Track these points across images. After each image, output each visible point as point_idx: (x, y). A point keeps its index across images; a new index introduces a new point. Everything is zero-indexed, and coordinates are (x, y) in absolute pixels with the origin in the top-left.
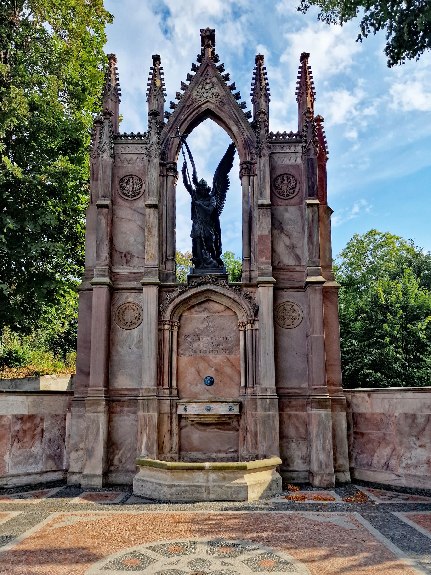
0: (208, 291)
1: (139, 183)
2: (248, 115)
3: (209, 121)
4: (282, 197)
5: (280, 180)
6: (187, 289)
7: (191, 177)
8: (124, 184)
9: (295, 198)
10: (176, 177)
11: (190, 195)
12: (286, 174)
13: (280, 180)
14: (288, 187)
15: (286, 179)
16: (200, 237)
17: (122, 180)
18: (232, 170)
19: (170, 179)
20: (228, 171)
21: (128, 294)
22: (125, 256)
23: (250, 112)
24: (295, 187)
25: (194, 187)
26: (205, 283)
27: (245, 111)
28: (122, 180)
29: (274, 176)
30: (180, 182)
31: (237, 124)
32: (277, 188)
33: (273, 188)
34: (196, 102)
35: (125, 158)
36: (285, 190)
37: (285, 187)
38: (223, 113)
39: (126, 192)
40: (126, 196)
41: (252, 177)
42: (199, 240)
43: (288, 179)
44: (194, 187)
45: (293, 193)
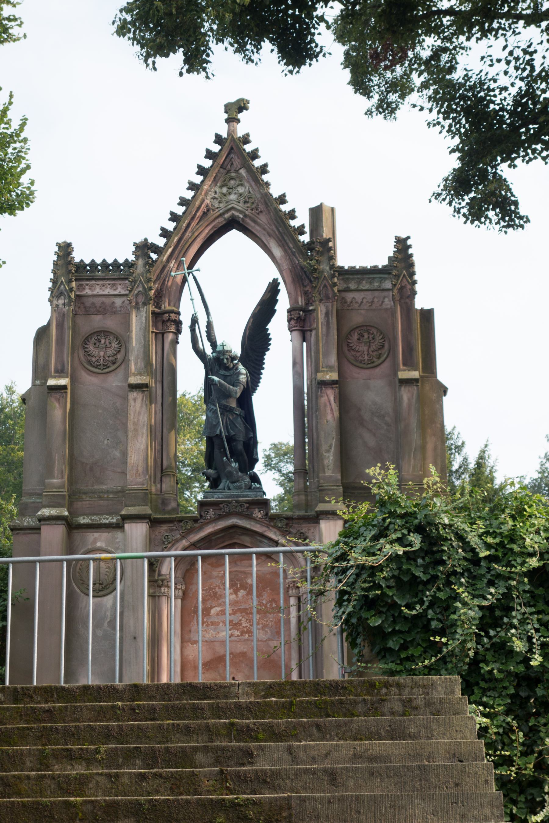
0: (234, 527)
1: (115, 344)
2: (301, 230)
3: (234, 235)
4: (361, 365)
5: (356, 336)
6: (197, 525)
7: (204, 334)
8: (91, 347)
9: (382, 366)
10: (179, 331)
11: (202, 365)
12: (366, 326)
13: (356, 336)
14: (369, 347)
15: (366, 336)
16: (219, 436)
17: (86, 341)
18: (273, 320)
19: (170, 337)
20: (268, 321)
21: (96, 535)
22: (91, 469)
23: (303, 226)
24: (383, 346)
25: (209, 351)
26: (229, 515)
27: (295, 223)
28: (86, 341)
29: (345, 330)
30: (185, 337)
31: (282, 244)
32: (351, 349)
33: (345, 349)
34: (213, 210)
35: (93, 303)
36: (366, 353)
37: (365, 348)
38: (257, 227)
39: (94, 359)
40: (93, 367)
41: (309, 333)
42: (216, 442)
43: (369, 333)
44: (209, 351)
45: (379, 358)
